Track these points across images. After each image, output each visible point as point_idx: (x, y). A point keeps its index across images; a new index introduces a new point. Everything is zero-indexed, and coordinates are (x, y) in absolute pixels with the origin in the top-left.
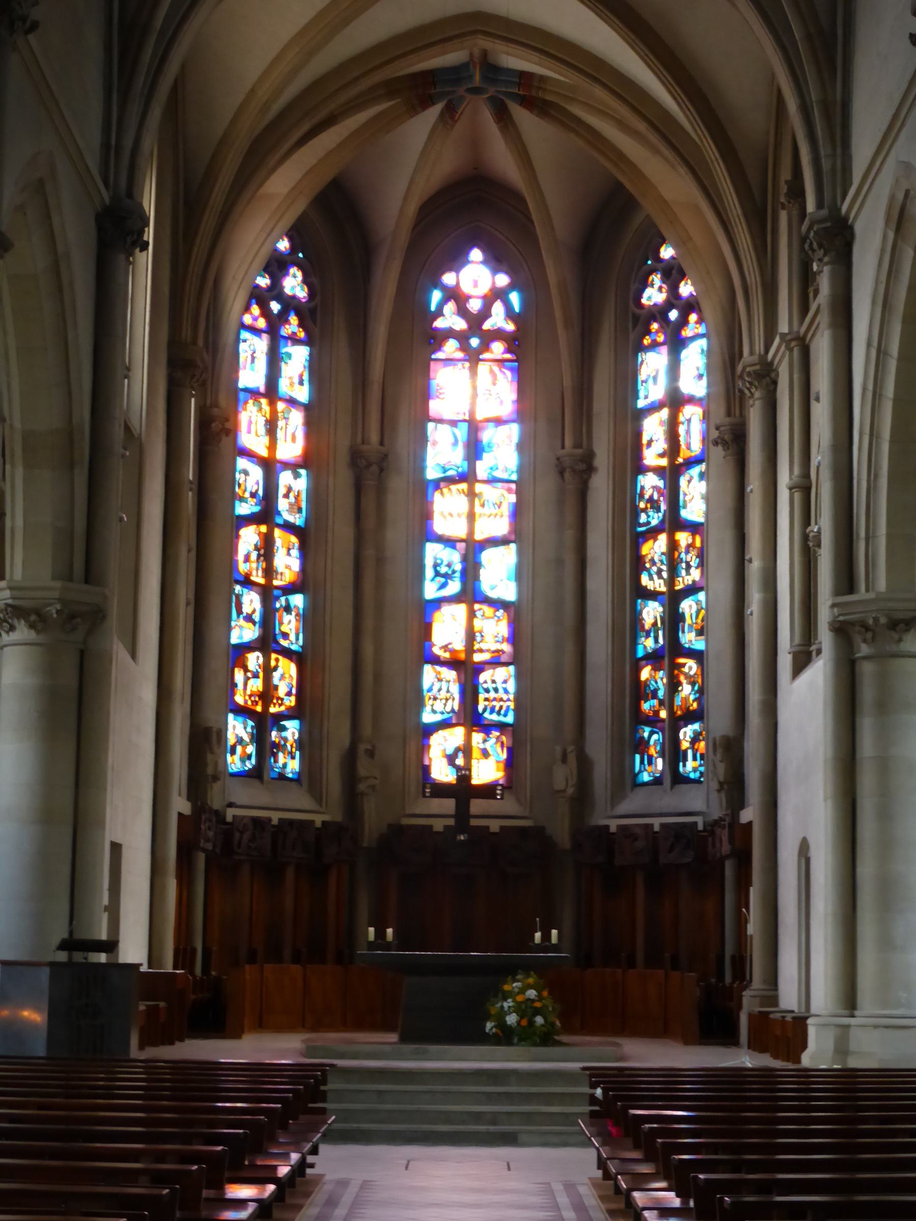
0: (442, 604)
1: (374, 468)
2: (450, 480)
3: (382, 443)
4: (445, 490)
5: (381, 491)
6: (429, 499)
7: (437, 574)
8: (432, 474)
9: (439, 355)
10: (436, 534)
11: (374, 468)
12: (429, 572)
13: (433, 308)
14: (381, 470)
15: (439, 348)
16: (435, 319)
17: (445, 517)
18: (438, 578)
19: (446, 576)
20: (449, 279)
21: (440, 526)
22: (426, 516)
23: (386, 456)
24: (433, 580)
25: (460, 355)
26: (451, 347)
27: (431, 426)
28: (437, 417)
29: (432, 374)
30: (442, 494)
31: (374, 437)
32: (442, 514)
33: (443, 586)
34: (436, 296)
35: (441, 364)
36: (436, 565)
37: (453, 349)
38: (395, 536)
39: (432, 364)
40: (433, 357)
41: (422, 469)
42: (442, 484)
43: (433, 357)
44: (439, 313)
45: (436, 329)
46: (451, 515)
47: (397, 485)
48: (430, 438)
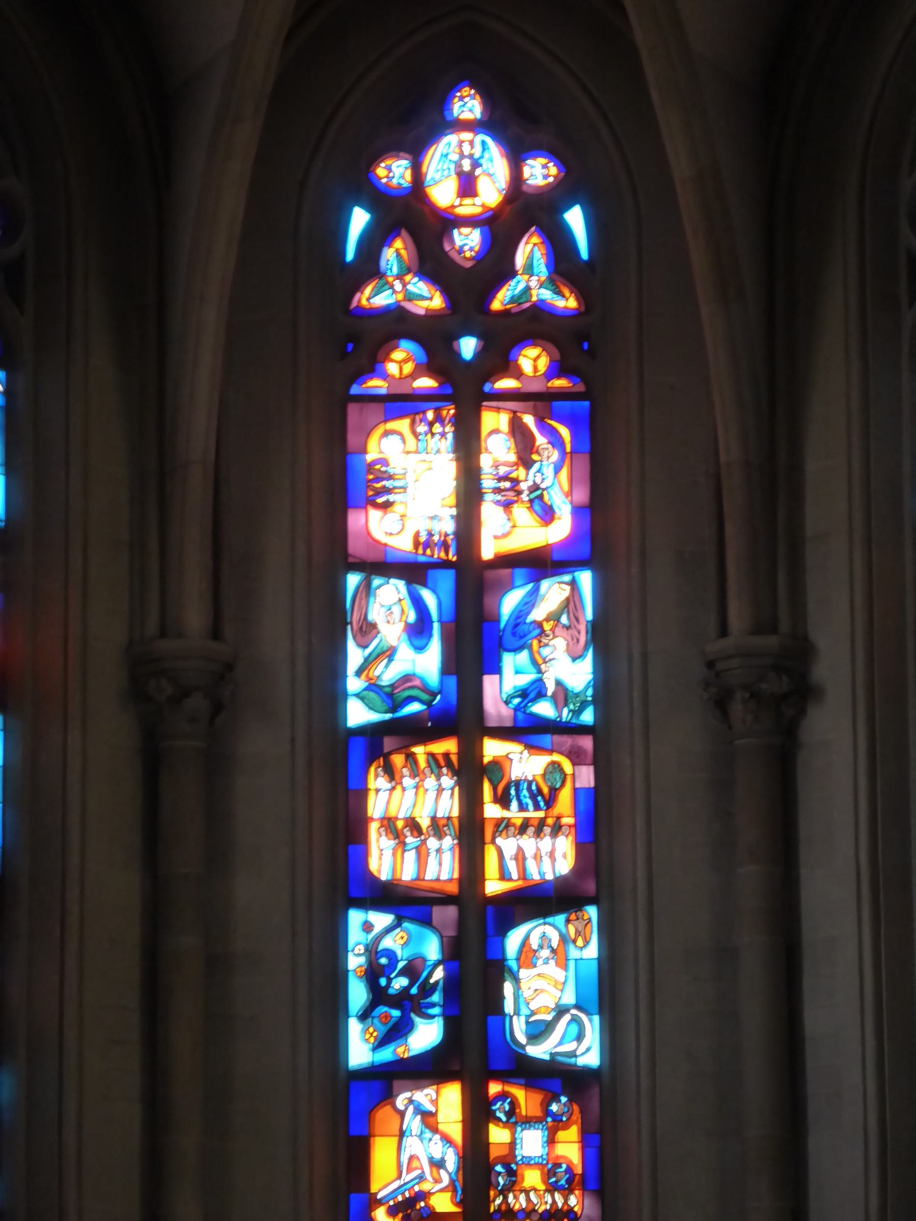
0: (396, 1084)
1: (197, 703)
2: (412, 731)
3: (216, 633)
4: (398, 760)
5: (216, 765)
6: (353, 784)
7: (378, 996)
8: (358, 714)
9: (377, 385)
10: (375, 880)
11: (197, 703)
12: (358, 994)
13: (350, 254)
14: (217, 707)
15: (373, 365)
16: (358, 287)
17: (398, 835)
18: (382, 1009)
19: (403, 1001)
20: (395, 172)
21: (383, 860)
22: (350, 829)
23: (229, 667)
24: (364, 1016)
25: (426, 383)
26: (401, 361)
27: (353, 580)
28: (372, 556)
29: (352, 440)
30: (390, 772)
31: (195, 618)
32: (388, 823)
33: (398, 1031)
34: (359, 220)
35: (376, 410)
36: (373, 974)
37: (408, 368)
38: (259, 893)
39: (353, 410)
40: (355, 390)
41: (335, 698)
42: (388, 743)
43: (355, 390)
44: (368, 268)
45: (360, 310)
46: (413, 825)
47: (264, 751)
48: (355, 618)
